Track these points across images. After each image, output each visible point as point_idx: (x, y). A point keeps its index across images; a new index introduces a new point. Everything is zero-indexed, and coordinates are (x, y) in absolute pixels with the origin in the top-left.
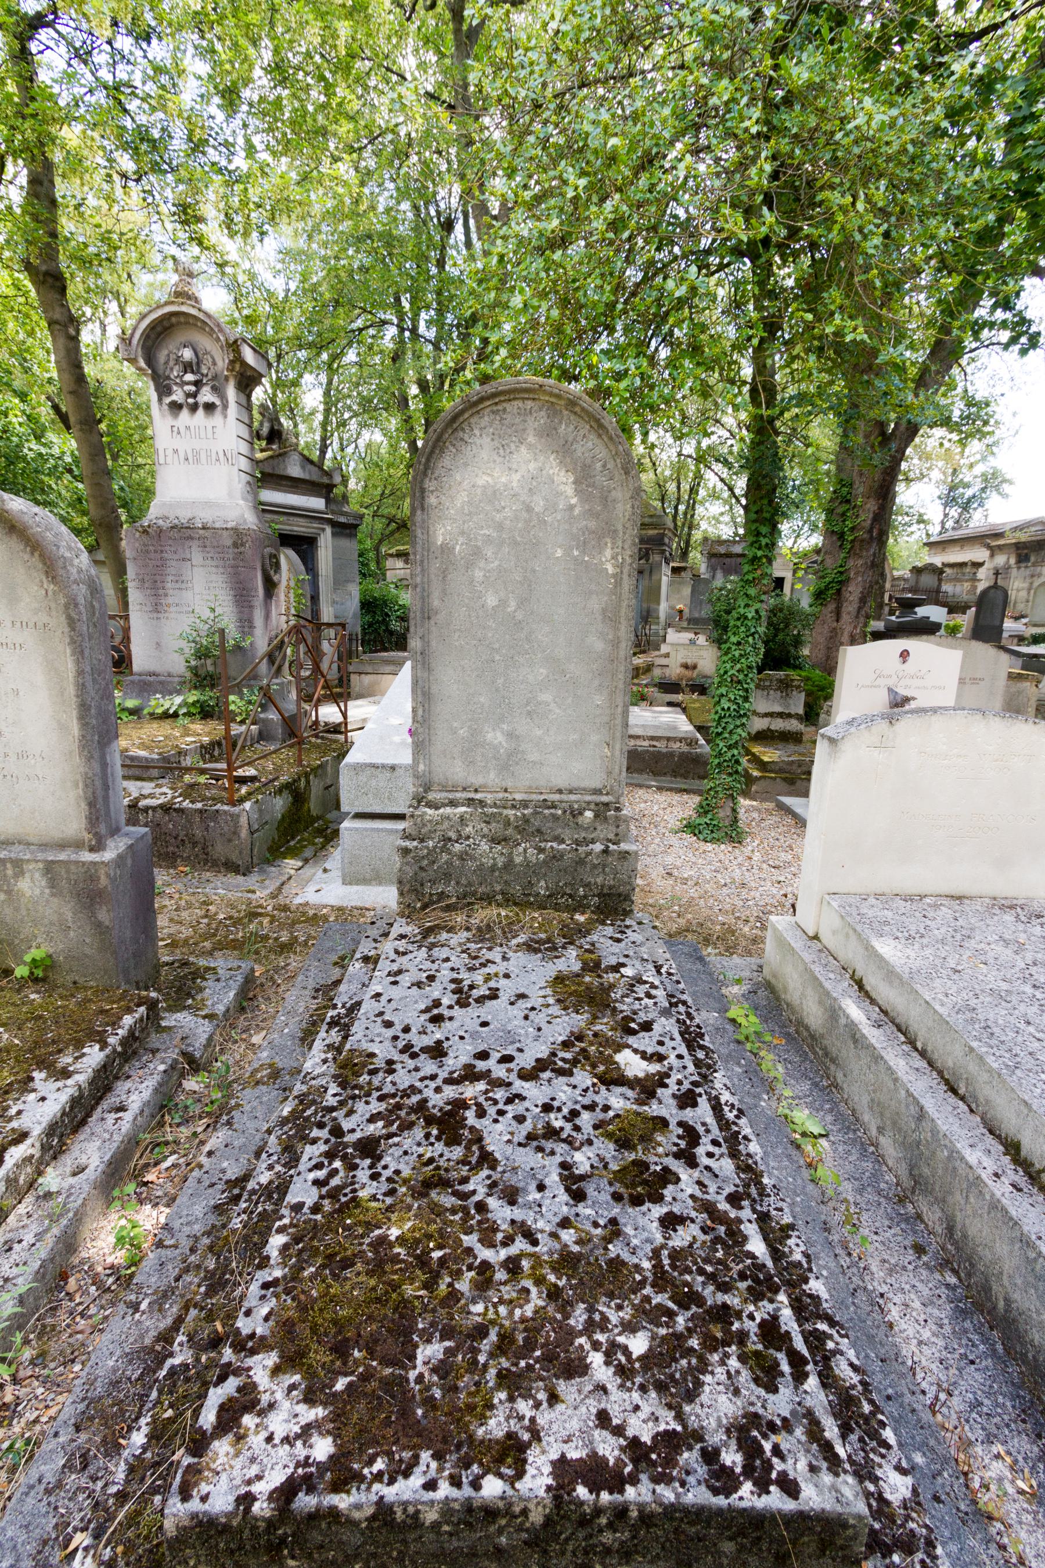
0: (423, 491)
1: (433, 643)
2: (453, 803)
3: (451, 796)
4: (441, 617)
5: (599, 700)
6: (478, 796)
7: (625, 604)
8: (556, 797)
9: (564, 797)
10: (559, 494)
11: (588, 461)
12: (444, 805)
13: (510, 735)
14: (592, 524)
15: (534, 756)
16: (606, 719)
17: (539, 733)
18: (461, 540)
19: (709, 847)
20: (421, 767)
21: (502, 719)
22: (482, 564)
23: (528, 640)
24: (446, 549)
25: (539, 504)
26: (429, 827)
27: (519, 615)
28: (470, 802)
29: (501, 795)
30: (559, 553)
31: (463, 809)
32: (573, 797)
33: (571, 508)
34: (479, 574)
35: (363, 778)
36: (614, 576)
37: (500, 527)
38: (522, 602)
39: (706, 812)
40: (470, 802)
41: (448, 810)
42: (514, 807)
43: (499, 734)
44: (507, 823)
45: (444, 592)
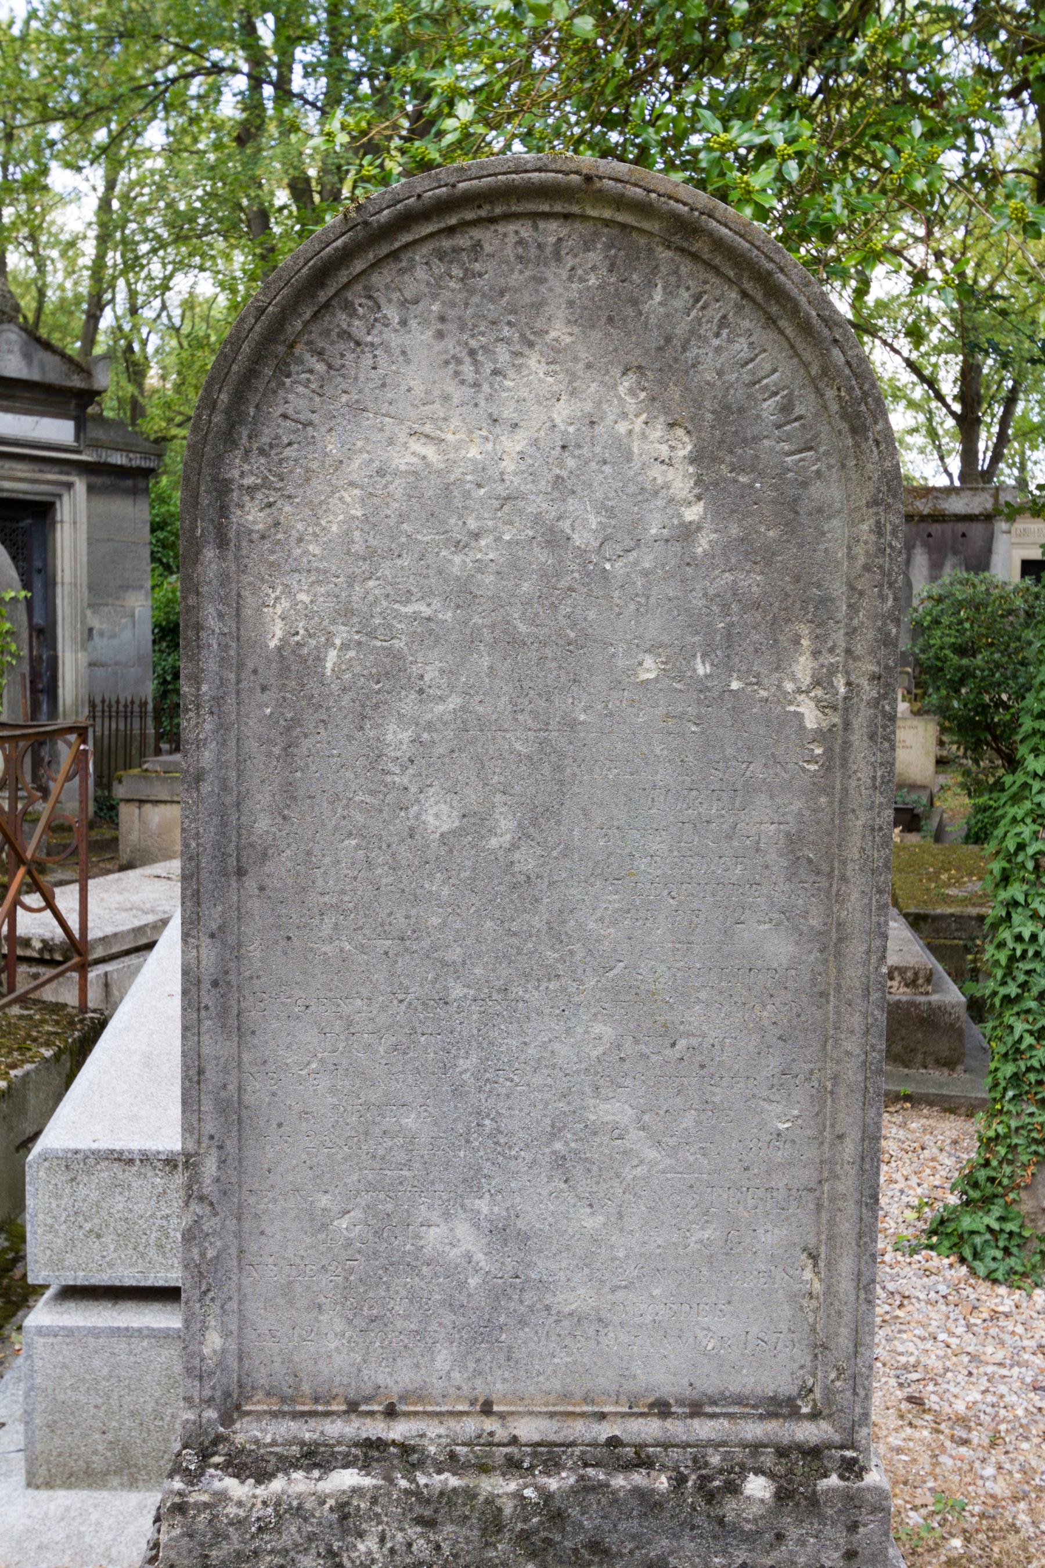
0: (223, 488)
1: (254, 950)
2: (316, 1458)
3: (308, 1432)
4: (280, 868)
5: (781, 1116)
6: (398, 1431)
7: (859, 822)
8: (650, 1429)
9: (676, 1429)
10: (648, 493)
11: (738, 395)
12: (287, 1465)
13: (502, 1233)
14: (752, 582)
15: (576, 1297)
16: (806, 1176)
17: (593, 1223)
18: (341, 634)
19: (1004, 1298)
20: (214, 1341)
21: (473, 1181)
22: (409, 704)
23: (555, 935)
24: (296, 664)
25: (585, 526)
26: (235, 1542)
27: (526, 861)
28: (370, 1453)
29: (470, 1427)
30: (649, 669)
31: (346, 1479)
32: (704, 1429)
33: (687, 533)
34: (397, 736)
35: (89, 1190)
36: (822, 736)
37: (463, 593)
38: (536, 819)
39: (987, 1201)
40: (370, 1453)
41: (297, 1484)
42: (513, 1465)
43: (463, 1230)
44: (493, 1523)
45: (289, 792)
